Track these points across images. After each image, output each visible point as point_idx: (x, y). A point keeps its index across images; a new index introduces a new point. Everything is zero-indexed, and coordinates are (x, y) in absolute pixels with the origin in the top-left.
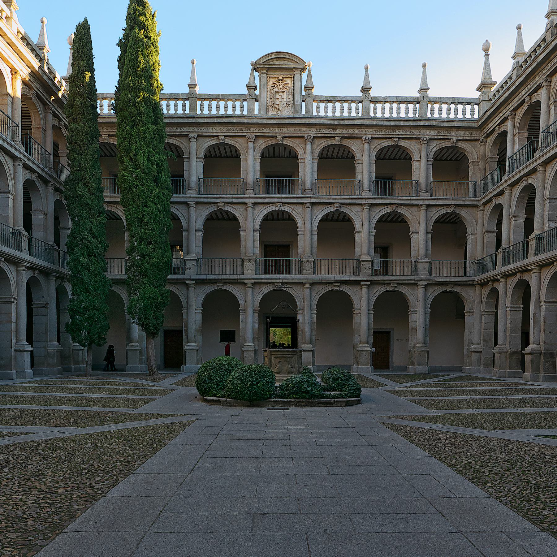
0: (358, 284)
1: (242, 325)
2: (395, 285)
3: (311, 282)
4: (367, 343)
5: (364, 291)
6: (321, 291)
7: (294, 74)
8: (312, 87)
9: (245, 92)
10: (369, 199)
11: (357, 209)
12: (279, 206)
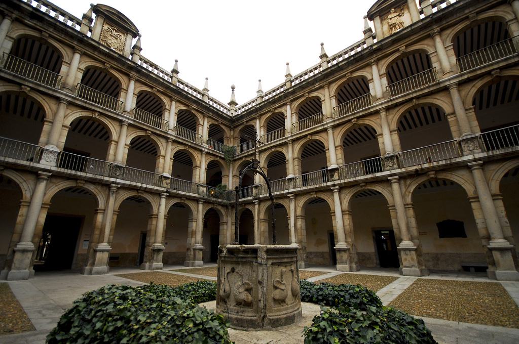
0: (158, 194)
1: (19, 219)
2: (185, 199)
3: (119, 186)
4: (161, 243)
5: (163, 201)
6: (125, 195)
7: (127, 34)
8: (140, 49)
9: (80, 17)
10: (173, 136)
11: (163, 141)
12: (97, 114)
